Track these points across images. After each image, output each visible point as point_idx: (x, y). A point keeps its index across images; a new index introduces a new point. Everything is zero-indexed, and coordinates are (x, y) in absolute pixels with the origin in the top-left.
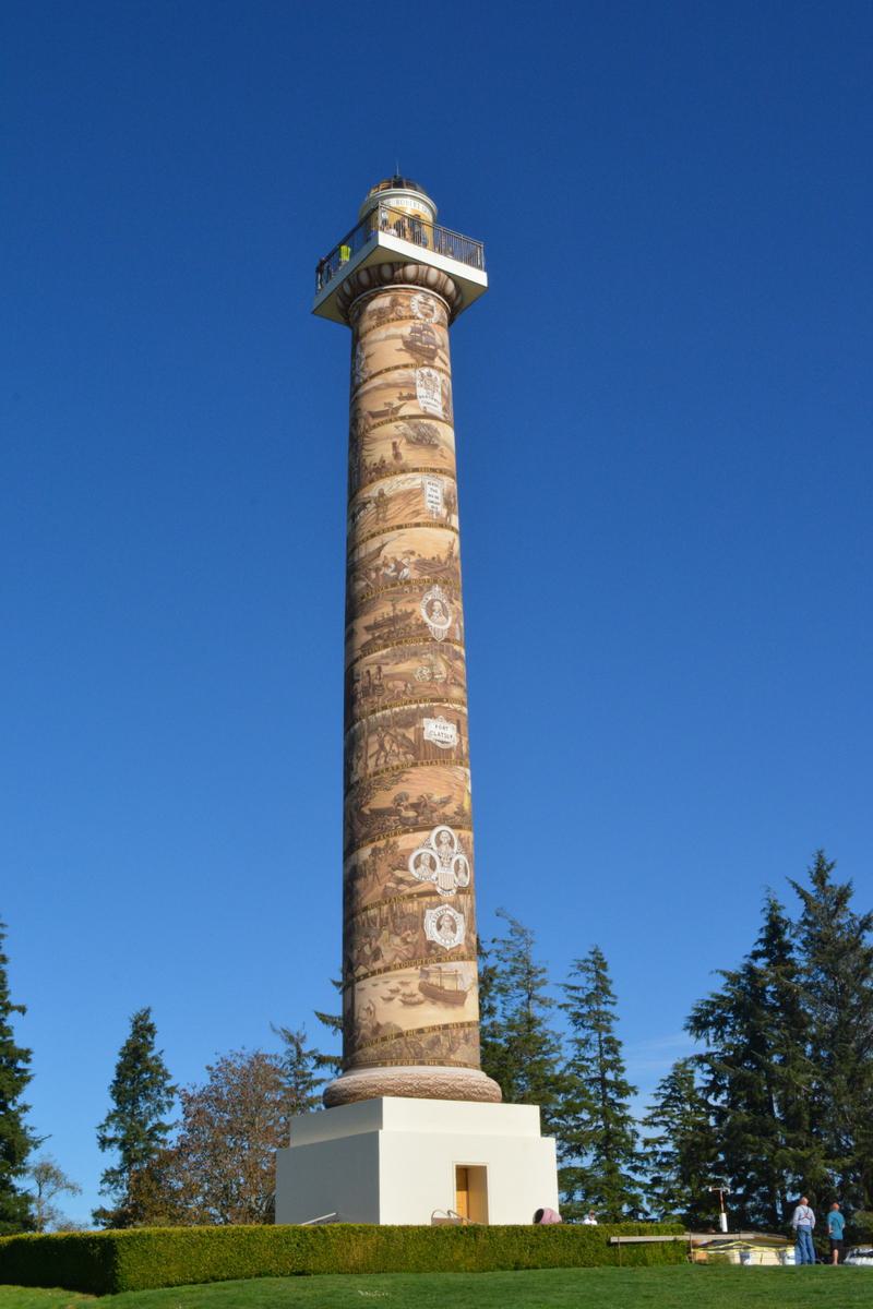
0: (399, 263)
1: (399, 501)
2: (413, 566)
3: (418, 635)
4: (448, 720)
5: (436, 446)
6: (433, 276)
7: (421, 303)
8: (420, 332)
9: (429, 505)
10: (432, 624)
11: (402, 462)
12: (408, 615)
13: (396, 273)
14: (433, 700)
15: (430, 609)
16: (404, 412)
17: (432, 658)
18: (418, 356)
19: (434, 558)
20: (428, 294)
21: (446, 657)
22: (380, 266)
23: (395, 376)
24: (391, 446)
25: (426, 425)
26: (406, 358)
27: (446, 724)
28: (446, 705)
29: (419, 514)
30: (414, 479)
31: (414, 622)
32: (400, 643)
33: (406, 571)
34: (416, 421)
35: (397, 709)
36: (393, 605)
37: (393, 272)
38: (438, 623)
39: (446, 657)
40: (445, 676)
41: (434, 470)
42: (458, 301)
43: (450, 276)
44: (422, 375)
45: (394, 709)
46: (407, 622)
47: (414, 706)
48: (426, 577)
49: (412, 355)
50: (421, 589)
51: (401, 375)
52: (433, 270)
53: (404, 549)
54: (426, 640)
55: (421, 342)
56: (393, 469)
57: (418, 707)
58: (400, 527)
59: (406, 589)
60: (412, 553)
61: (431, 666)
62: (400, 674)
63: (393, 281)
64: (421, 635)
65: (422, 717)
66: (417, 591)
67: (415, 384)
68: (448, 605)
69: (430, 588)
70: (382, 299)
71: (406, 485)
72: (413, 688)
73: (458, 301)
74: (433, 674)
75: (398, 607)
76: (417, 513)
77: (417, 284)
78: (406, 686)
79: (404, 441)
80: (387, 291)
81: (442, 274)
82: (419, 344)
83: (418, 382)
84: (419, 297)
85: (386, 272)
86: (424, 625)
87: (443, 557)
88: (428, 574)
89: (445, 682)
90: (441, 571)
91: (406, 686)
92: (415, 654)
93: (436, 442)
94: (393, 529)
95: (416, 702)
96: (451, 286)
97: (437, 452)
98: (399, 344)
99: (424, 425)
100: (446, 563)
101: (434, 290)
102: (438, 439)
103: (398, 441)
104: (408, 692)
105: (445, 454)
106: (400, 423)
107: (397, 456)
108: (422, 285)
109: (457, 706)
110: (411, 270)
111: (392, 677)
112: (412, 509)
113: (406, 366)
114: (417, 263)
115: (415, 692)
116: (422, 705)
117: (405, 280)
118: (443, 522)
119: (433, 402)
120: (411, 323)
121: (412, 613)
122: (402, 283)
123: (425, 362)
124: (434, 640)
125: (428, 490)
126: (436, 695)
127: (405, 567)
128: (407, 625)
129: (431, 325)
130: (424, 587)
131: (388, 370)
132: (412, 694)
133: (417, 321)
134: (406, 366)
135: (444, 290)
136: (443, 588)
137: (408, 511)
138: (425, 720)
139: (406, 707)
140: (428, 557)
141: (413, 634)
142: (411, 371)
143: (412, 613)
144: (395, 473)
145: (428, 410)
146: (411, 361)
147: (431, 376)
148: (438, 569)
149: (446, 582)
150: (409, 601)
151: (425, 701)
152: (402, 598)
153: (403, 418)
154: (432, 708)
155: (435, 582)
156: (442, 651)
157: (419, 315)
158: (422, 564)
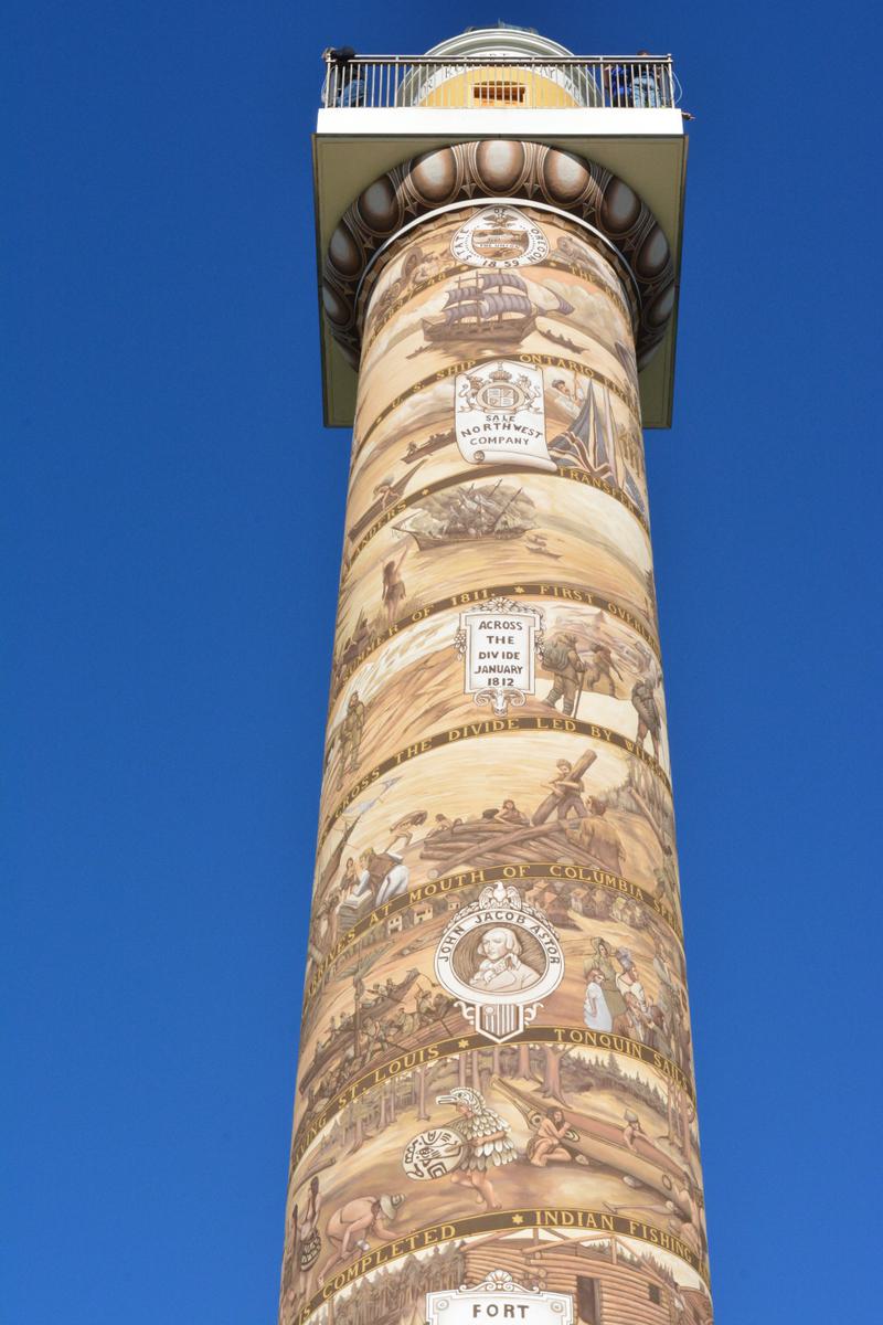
0: (400, 166)
1: (392, 699)
2: (417, 853)
3: (423, 1042)
4: (528, 1282)
5: (517, 532)
6: (499, 159)
7: (482, 234)
8: (477, 294)
9: (481, 681)
10: (479, 999)
11: (401, 603)
12: (394, 994)
13: (400, 192)
14: (465, 1228)
15: (469, 957)
16: (409, 490)
17: (466, 1095)
18: (463, 346)
19: (489, 814)
20: (497, 207)
21: (527, 1086)
22: (361, 199)
23: (404, 414)
24: (380, 577)
25: (482, 491)
26: (435, 361)
27: (517, 1296)
28: (527, 1233)
29: (446, 711)
30: (433, 631)
31: (410, 1007)
32: (370, 1082)
33: (396, 875)
34: (450, 491)
35: (345, 1292)
36: (358, 984)
37: (392, 192)
38: (505, 990)
39: (527, 1086)
40: (521, 1142)
41: (506, 591)
42: (609, 207)
43: (556, 143)
44: (476, 384)
45: (337, 1297)
46: (389, 1016)
47: (397, 1264)
48: (462, 869)
49: (446, 350)
50: (440, 908)
51: (413, 406)
52: (494, 145)
53: (396, 818)
54: (452, 1047)
55: (477, 312)
56: (380, 632)
57: (409, 1265)
58: (386, 766)
59: (396, 922)
60: (419, 819)
61: (466, 1120)
62: (362, 1176)
63: (400, 216)
64: (433, 1037)
65: (419, 1293)
66: (428, 916)
67: (453, 409)
68: (544, 935)
69: (469, 899)
70: (389, 273)
71: (410, 653)
72: (396, 1206)
73: (609, 207)
74: (470, 1145)
75: (369, 984)
76: (440, 710)
77: (463, 196)
78: (376, 1206)
79: (415, 548)
80: (395, 248)
81: (528, 147)
82: (465, 320)
83: (461, 402)
84: (479, 223)
85: (378, 204)
86: (449, 1005)
87: (529, 806)
88: (467, 862)
89: (524, 1161)
90: (520, 843)
91: (376, 1206)
92: (411, 1100)
93: (516, 522)
94: (370, 778)
95: (405, 1248)
96: (568, 171)
97: (521, 546)
98: (419, 339)
99: (471, 494)
100: (541, 820)
101: (522, 194)
102: (523, 515)
103: (395, 557)
104: (380, 1225)
105: (550, 547)
106: (409, 512)
107: (392, 591)
108: (478, 194)
109: (574, 1234)
110: (433, 169)
111: (340, 1197)
112: (424, 704)
113: (431, 380)
114: (444, 142)
115: (405, 1215)
116: (423, 1255)
117: (428, 200)
118: (539, 712)
119: (513, 434)
120: (451, 284)
121: (406, 985)
122: (422, 210)
123: (489, 353)
124: (478, 1041)
125: (479, 642)
126: (479, 1208)
127: (396, 862)
128: (391, 1024)
129: (516, 272)
130: (443, 898)
131: (389, 409)
132: (394, 1224)
133: (472, 274)
134: (431, 380)
135: (548, 182)
136: (524, 889)
137: (412, 714)
138: (432, 1297)
139: (371, 1276)
140: (470, 813)
141: (404, 1045)
142: (443, 388)
143: (406, 985)
144: (386, 637)
145: (490, 456)
146: (449, 362)
147: (506, 378)
148: (504, 839)
149: (536, 871)
150: (401, 954)
151: (437, 1236)
152: (379, 953)
153: (410, 501)
154: (463, 1255)
155: (494, 875)
156: (514, 1071)
157: (477, 260)
158: (449, 840)
